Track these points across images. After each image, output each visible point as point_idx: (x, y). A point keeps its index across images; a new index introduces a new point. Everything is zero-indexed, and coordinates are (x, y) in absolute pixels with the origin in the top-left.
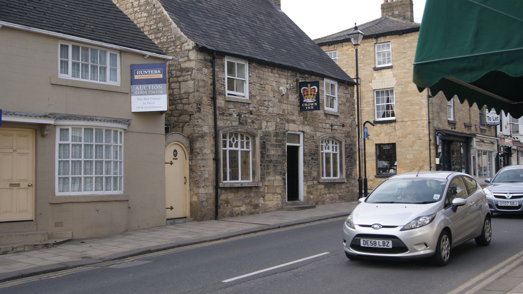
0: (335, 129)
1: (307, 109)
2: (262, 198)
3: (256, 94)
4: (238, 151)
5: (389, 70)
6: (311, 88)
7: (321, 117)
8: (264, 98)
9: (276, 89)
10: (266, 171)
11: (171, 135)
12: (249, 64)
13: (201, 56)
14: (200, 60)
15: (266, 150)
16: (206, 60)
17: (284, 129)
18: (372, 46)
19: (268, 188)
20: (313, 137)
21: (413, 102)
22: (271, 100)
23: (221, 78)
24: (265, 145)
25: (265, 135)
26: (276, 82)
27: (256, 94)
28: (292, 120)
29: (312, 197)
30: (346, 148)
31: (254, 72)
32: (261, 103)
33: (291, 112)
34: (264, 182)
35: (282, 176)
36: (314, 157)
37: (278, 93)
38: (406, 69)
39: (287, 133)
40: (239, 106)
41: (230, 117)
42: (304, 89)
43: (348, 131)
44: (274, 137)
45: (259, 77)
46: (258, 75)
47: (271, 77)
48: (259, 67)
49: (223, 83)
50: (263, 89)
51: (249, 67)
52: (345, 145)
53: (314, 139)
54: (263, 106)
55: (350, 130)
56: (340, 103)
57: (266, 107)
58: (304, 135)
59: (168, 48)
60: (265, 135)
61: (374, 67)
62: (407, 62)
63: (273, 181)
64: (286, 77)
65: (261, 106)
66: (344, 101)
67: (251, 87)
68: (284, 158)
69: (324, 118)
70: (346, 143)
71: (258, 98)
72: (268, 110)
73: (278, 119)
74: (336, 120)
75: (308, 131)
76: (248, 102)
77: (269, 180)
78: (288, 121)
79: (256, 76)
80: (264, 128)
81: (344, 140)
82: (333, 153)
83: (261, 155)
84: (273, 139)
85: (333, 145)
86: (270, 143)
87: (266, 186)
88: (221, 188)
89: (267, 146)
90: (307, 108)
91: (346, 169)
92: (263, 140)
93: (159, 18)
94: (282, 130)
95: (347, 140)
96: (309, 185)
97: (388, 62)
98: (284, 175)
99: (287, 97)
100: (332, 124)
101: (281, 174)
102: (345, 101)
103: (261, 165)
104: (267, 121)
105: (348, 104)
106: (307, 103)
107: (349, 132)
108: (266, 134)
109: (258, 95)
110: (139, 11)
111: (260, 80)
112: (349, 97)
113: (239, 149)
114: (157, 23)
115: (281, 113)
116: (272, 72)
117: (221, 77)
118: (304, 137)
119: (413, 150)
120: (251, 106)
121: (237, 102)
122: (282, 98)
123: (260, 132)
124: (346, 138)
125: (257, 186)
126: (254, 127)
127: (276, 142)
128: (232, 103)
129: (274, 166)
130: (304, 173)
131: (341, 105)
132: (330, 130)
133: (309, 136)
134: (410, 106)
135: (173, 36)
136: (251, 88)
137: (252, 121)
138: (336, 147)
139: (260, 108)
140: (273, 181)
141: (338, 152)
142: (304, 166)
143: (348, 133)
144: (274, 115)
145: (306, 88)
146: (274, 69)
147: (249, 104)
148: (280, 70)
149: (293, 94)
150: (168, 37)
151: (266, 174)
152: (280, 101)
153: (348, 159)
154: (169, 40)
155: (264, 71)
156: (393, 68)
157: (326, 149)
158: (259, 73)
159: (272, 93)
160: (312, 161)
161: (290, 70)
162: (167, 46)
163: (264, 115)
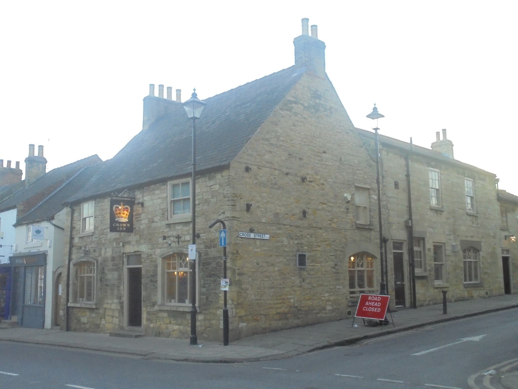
1: (118, 229)
7: (161, 230)
17: (120, 252)
25: (104, 261)
29: (152, 325)
36: (153, 279)
50: (104, 219)
54: (104, 235)
68: (120, 281)
69: (167, 230)
71: (99, 228)
73: (115, 243)
80: (103, 254)
84: (110, 264)
87: (106, 308)
89: (105, 271)
90: (119, 229)
96: (149, 311)
100: (178, 235)
101: (118, 297)
102: (210, 196)
104: (105, 249)
107: (214, 239)
108: (105, 260)
115: (118, 237)
127: (113, 266)
133: (146, 256)
139: (101, 237)
143: (212, 241)
144: (112, 240)
147: (92, 236)
153: (211, 279)
160: (150, 284)
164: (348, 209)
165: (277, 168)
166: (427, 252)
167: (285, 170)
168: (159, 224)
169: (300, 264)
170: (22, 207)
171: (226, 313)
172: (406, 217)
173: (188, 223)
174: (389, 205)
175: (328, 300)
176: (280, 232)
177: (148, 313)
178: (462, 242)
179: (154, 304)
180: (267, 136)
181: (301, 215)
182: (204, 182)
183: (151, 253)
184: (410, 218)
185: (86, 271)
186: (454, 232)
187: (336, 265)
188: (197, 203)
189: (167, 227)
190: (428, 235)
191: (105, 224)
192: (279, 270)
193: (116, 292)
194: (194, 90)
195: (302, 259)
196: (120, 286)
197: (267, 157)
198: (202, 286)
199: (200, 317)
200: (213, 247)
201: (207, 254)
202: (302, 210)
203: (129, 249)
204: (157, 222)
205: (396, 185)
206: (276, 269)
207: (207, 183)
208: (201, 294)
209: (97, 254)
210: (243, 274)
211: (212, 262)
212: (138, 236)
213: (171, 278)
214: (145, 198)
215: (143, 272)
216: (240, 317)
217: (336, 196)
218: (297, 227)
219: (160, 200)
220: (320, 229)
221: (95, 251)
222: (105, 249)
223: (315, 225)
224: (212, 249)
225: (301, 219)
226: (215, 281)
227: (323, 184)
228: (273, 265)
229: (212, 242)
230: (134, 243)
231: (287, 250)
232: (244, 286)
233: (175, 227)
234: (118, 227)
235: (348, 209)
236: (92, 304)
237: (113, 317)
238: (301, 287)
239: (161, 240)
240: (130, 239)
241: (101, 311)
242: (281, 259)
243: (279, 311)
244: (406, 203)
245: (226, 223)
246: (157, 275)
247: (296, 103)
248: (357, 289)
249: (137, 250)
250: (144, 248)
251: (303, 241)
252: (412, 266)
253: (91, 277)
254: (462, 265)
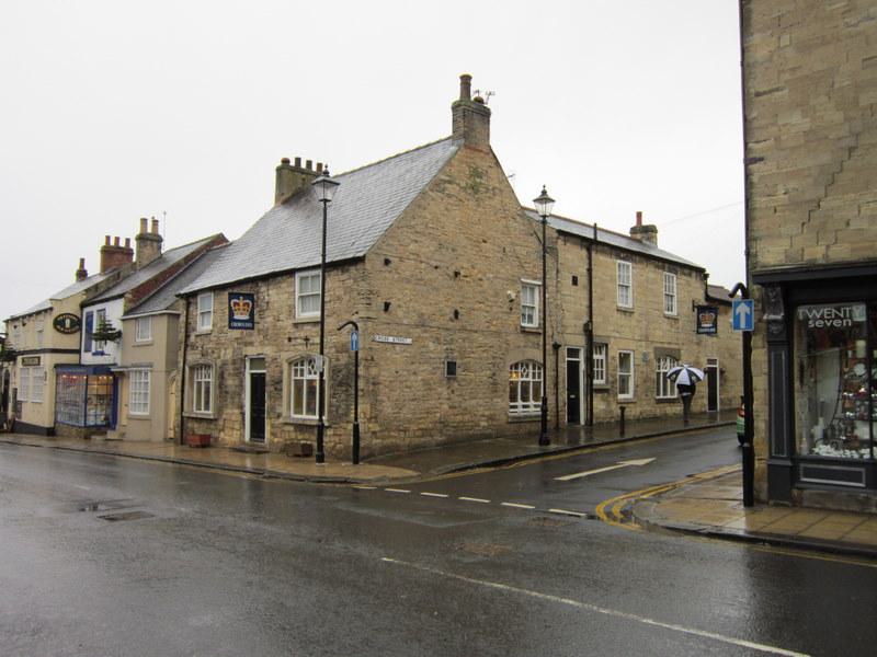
29: (276, 440)
69: (294, 330)
78: (246, 344)
108: (225, 364)
129: (232, 398)
140: (233, 414)
164: (511, 309)
165: (423, 259)
166: (609, 360)
167: (435, 264)
168: (285, 323)
169: (448, 374)
170: (130, 296)
171: (356, 428)
172: (585, 319)
173: (317, 323)
174: (564, 305)
175: (483, 416)
176: (425, 335)
177: (273, 426)
178: (656, 349)
179: (279, 416)
180: (412, 223)
181: (452, 316)
184: (591, 321)
186: (646, 338)
187: (494, 374)
188: (327, 299)
190: (612, 340)
192: (422, 380)
193: (236, 400)
195: (451, 368)
197: (412, 247)
198: (333, 396)
199: (329, 432)
201: (338, 360)
202: (453, 311)
203: (251, 351)
205: (575, 281)
206: (420, 378)
208: (331, 405)
209: (215, 355)
210: (379, 384)
213: (299, 384)
214: (270, 292)
215: (267, 379)
216: (374, 433)
217: (497, 295)
218: (447, 329)
219: (287, 295)
220: (476, 332)
221: (213, 352)
222: (226, 349)
223: (469, 328)
225: (451, 320)
227: (481, 280)
228: (415, 373)
230: (256, 344)
231: (432, 356)
232: (379, 398)
235: (511, 309)
236: (210, 413)
237: (233, 429)
238: (449, 399)
239: (286, 341)
240: (253, 339)
241: (221, 423)
242: (426, 367)
243: (422, 426)
244: (586, 303)
245: (359, 324)
246: (282, 381)
247: (450, 182)
248: (520, 403)
250: (268, 351)
251: (453, 347)
252: (590, 376)
254: (655, 377)
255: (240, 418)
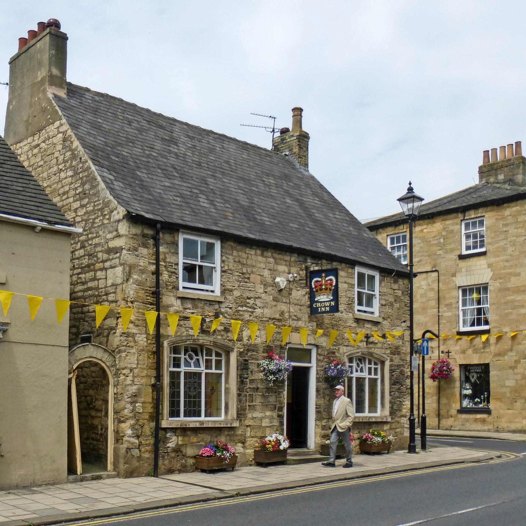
0: (372, 343)
2: (240, 445)
3: (234, 288)
4: (200, 374)
5: (482, 258)
6: (327, 279)
7: (348, 324)
8: (248, 294)
9: (269, 280)
10: (248, 404)
11: (82, 348)
12: (222, 242)
13: (136, 230)
14: (135, 235)
15: (249, 372)
16: (144, 236)
18: (457, 224)
19: (251, 429)
20: (334, 353)
21: (516, 304)
22: (259, 298)
23: (172, 263)
24: (247, 364)
26: (270, 270)
27: (234, 288)
28: (296, 327)
30: (392, 371)
31: (229, 254)
32: (242, 302)
33: (295, 316)
34: (244, 420)
35: (276, 411)
37: (273, 286)
38: (506, 255)
39: (287, 347)
40: (202, 305)
41: (186, 322)
42: (317, 281)
43: (397, 345)
44: (263, 352)
45: (239, 262)
46: (237, 260)
47: (260, 262)
48: (239, 247)
49: (174, 270)
50: (246, 280)
51: (222, 247)
52: (391, 366)
53: (336, 357)
54: (246, 306)
55: (401, 343)
56: (384, 303)
57: (251, 308)
58: (317, 351)
59: (94, 219)
60: (248, 350)
61: (458, 253)
62: (509, 245)
63: (261, 419)
64: (288, 263)
65: (242, 306)
66: (390, 300)
67: (225, 277)
69: (354, 325)
70: (391, 363)
72: (255, 312)
74: (374, 328)
75: (324, 344)
76: (218, 299)
77: (253, 418)
79: (235, 261)
80: (247, 338)
81: (389, 358)
82: (369, 379)
83: (239, 380)
85: (370, 366)
86: (257, 362)
87: (247, 426)
88: (165, 429)
89: (250, 367)
90: (321, 309)
91: (391, 402)
92: (245, 357)
93: (86, 176)
94: (278, 343)
95: (394, 358)
97: (482, 246)
98: (281, 409)
99: (289, 293)
102: (393, 300)
103: (239, 395)
105: (397, 305)
106: (321, 302)
107: (399, 346)
108: (250, 348)
109: (236, 289)
110: (64, 169)
111: (240, 267)
112: (400, 295)
113: (202, 369)
114: (83, 184)
115: (277, 316)
116: (262, 255)
117: (172, 261)
118: (318, 354)
119: (515, 374)
120: (223, 306)
121: (199, 299)
122: (280, 294)
123: (238, 344)
124: (392, 356)
125: (229, 426)
126: (228, 337)
128: (188, 301)
130: (316, 408)
131: (385, 305)
132: (365, 343)
133: (326, 353)
134: (512, 309)
135: (101, 201)
136: (225, 278)
137: (225, 328)
138: (376, 369)
139: (240, 308)
140: (261, 419)
141: (379, 376)
142: (317, 397)
143: (397, 348)
144: (264, 319)
145: (320, 279)
146: (267, 250)
147: (220, 303)
148: (277, 252)
149: (299, 289)
150: (96, 204)
151: (248, 408)
152: (275, 299)
154: (96, 208)
155: (248, 254)
156: (488, 254)
157: (357, 371)
158: (239, 256)
159: (262, 286)
161: (295, 253)
162: (93, 217)
163: (246, 319)
168: (344, 315)
182: (389, 284)
183: (333, 351)
185: (354, 370)
189: (355, 322)
191: (250, 290)
194: (410, 184)
196: (282, 392)
200: (398, 354)
204: (342, 313)
207: (392, 285)
211: (396, 369)
212: (315, 324)
219: (346, 286)
224: (396, 356)
226: (399, 389)
229: (397, 349)
233: (364, 324)
234: (319, 307)
249: (313, 342)
253: (195, 374)
255: (276, 423)
